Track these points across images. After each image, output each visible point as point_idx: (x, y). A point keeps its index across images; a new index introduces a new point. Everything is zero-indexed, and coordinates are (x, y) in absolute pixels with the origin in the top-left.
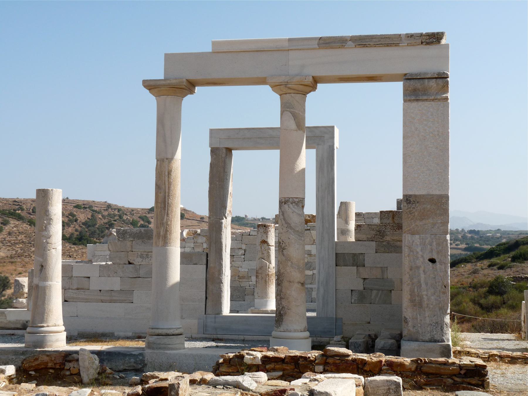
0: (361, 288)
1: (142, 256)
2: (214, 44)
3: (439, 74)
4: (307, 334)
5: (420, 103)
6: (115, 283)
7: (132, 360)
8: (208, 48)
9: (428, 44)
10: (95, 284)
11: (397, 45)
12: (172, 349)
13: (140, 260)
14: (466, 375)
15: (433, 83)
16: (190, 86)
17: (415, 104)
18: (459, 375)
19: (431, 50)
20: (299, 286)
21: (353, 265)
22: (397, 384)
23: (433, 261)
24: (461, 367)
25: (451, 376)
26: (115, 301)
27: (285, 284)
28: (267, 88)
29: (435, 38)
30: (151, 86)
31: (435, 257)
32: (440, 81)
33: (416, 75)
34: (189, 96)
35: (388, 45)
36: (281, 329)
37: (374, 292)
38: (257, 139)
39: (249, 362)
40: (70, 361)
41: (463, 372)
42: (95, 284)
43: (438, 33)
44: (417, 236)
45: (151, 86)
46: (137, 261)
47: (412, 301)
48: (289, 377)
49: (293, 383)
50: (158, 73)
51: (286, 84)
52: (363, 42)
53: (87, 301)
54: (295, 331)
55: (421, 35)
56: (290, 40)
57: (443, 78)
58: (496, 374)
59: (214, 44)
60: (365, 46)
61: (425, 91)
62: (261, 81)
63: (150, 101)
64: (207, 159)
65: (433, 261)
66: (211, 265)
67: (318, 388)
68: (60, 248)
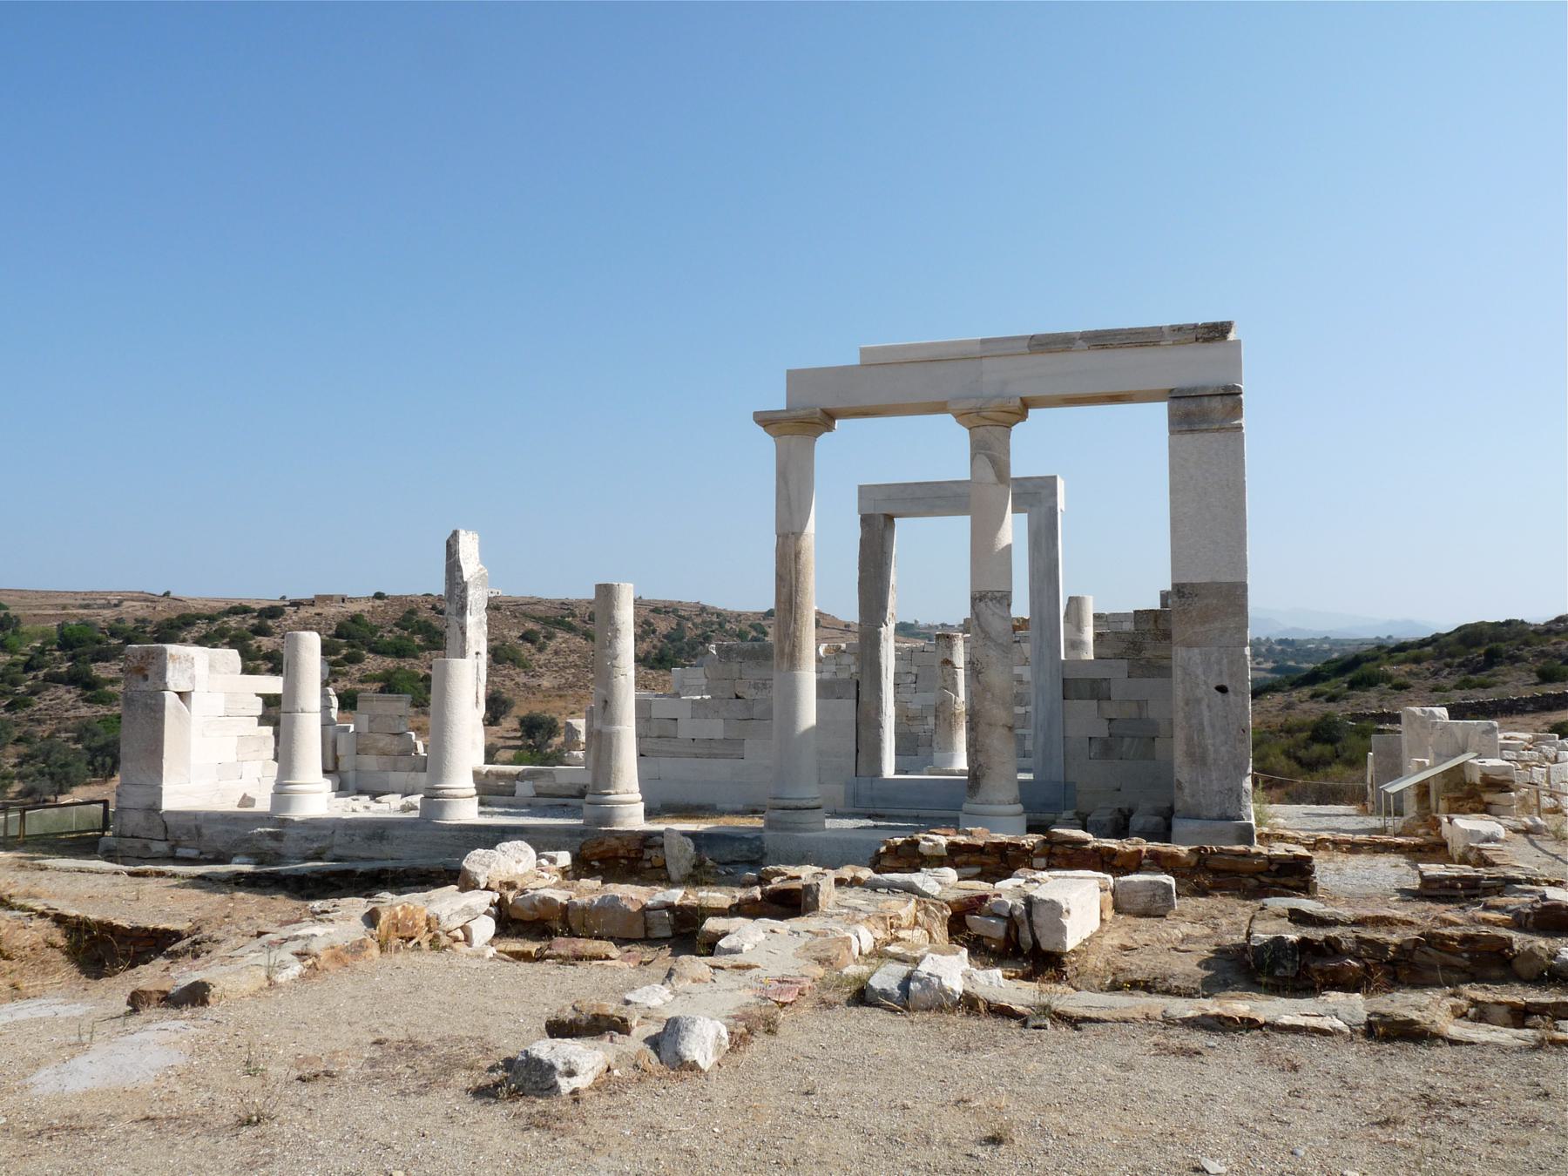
0: (1106, 734)
1: (755, 687)
2: (863, 351)
3: (1226, 388)
4: (1019, 808)
5: (1197, 435)
6: (715, 728)
7: (745, 847)
8: (854, 359)
9: (1206, 340)
10: (686, 729)
11: (1156, 344)
12: (806, 830)
13: (753, 691)
15: (1216, 403)
16: (826, 420)
17: (1188, 437)
18: (1267, 872)
19: (1213, 350)
20: (1005, 731)
21: (1092, 698)
22: (1168, 888)
23: (1222, 689)
24: (1271, 860)
25: (1255, 874)
26: (715, 756)
27: (982, 727)
28: (948, 419)
29: (1217, 332)
30: (767, 421)
31: (1226, 683)
32: (1229, 401)
33: (1190, 390)
34: (826, 434)
35: (1141, 345)
36: (978, 799)
37: (1127, 741)
38: (933, 499)
39: (927, 852)
40: (651, 847)
41: (1273, 868)
42: (686, 729)
43: (1222, 323)
44: (1196, 650)
45: (767, 421)
46: (750, 694)
47: (1190, 754)
48: (992, 876)
49: (998, 885)
50: (777, 401)
51: (978, 412)
52: (1101, 340)
53: (674, 755)
54: (1000, 803)
55: (1196, 326)
56: (983, 342)
57: (1232, 394)
58: (1326, 870)
59: (863, 351)
60: (1104, 347)
61: (1204, 417)
63: (766, 444)
64: (855, 533)
65: (1222, 689)
66: (864, 698)
67: (1039, 893)
68: (632, 673)
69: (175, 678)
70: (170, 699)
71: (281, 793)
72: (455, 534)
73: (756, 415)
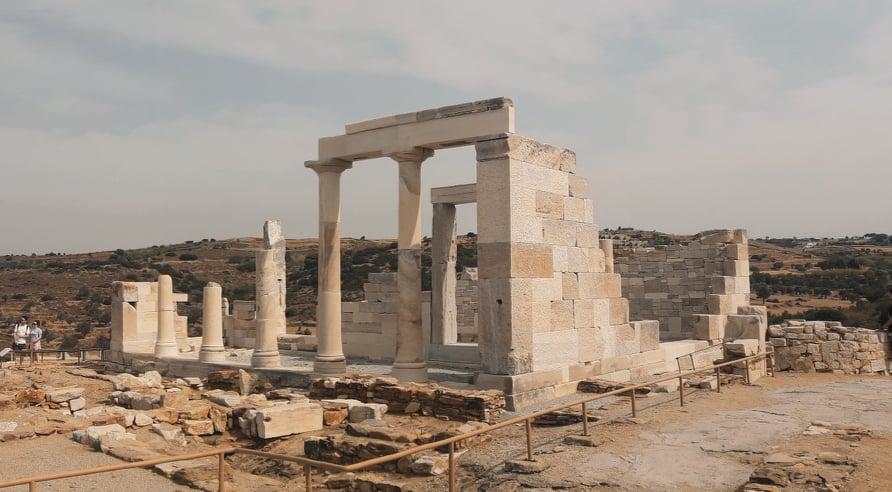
3: (500, 135)
8: (343, 132)
14: (468, 407)
15: (496, 143)
19: (492, 116)
24: (466, 399)
25: (458, 406)
28: (388, 160)
29: (496, 104)
33: (485, 137)
38: (466, 193)
39: (326, 386)
50: (314, 157)
55: (486, 102)
56: (396, 117)
61: (492, 150)
62: (378, 154)
66: (434, 302)
69: (128, 296)
70: (125, 305)
71: (157, 347)
72: (266, 223)
73: (306, 163)
